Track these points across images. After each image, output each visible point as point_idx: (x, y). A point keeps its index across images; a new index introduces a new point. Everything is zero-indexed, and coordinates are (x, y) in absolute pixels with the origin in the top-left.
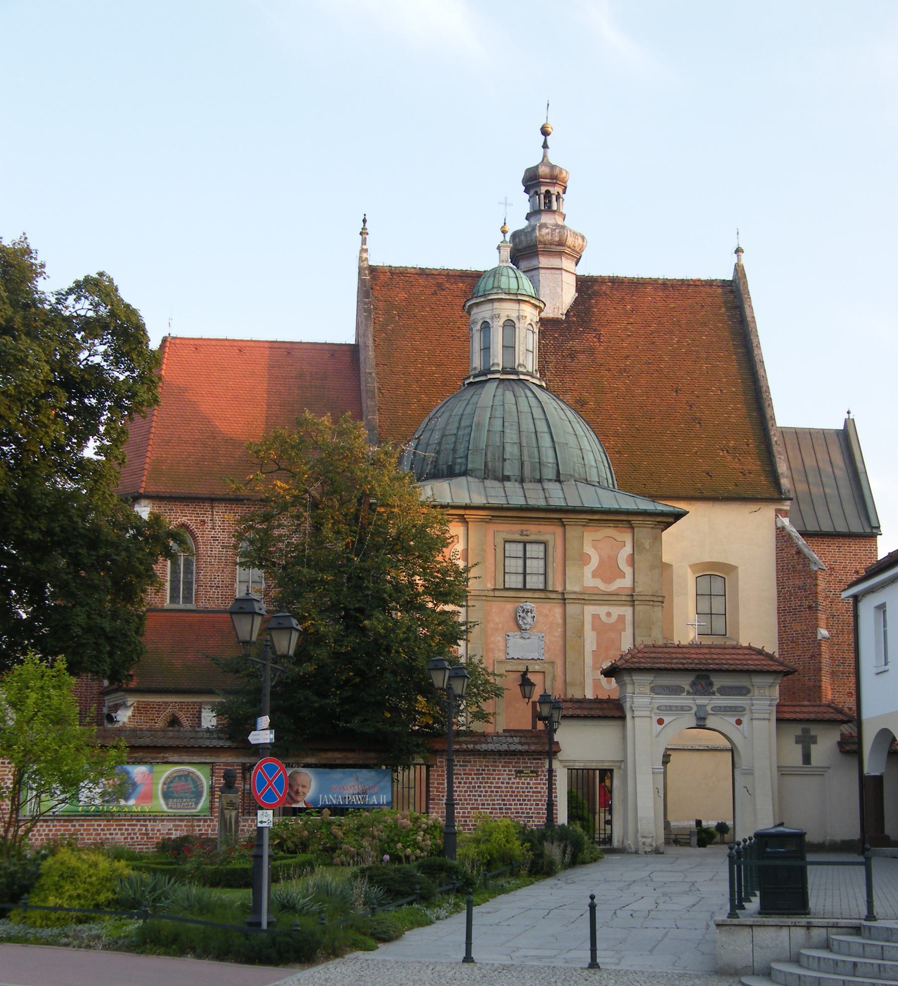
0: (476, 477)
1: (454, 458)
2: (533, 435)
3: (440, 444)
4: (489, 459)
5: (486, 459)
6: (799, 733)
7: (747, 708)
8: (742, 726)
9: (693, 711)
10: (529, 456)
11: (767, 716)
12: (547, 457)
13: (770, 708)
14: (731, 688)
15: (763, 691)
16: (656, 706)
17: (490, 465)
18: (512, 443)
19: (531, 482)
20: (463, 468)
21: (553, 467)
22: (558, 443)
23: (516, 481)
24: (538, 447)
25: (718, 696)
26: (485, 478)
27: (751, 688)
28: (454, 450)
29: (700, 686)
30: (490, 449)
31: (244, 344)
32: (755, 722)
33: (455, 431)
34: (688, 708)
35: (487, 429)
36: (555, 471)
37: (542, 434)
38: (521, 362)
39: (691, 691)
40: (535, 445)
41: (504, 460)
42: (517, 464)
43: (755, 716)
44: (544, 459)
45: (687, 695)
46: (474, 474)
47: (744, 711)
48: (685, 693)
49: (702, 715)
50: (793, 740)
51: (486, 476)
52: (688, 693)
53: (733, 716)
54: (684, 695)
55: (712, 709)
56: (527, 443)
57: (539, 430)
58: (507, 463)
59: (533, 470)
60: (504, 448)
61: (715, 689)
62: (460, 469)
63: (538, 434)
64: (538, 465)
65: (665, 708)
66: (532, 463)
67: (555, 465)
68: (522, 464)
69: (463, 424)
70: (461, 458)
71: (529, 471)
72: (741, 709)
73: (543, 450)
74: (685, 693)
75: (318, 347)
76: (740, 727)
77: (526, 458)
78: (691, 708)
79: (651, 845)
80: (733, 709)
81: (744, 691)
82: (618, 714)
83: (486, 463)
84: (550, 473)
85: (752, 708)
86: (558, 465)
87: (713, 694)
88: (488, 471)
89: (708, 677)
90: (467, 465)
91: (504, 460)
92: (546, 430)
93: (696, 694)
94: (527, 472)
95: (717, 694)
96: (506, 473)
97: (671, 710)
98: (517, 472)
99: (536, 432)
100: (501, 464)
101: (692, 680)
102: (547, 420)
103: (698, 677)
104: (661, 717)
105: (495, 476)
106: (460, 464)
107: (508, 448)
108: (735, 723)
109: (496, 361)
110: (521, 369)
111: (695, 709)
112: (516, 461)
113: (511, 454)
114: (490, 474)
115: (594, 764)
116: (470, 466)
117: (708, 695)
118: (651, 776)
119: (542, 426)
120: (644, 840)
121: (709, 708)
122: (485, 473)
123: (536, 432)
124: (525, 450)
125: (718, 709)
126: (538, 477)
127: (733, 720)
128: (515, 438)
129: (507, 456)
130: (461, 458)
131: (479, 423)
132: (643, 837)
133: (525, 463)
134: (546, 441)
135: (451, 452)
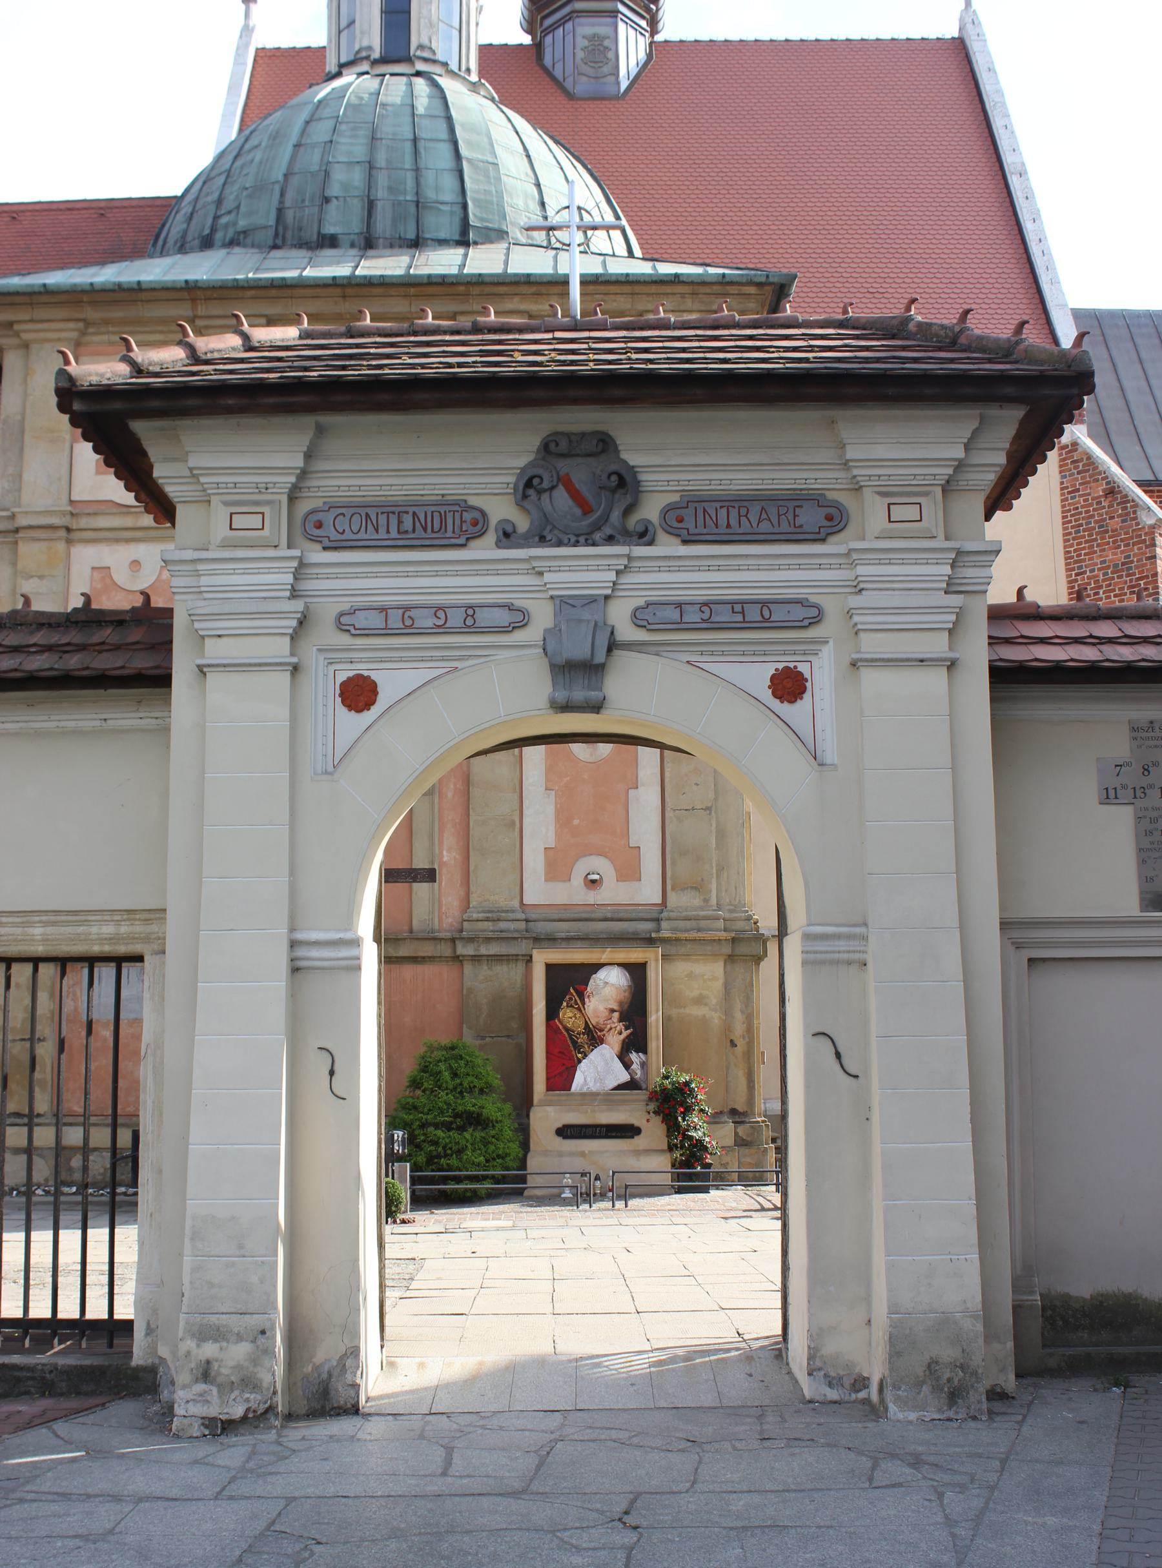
0: (253, 246)
1: (216, 218)
2: (408, 146)
3: (197, 199)
4: (288, 203)
5: (281, 202)
6: (1120, 747)
7: (831, 606)
8: (803, 705)
9: (533, 634)
10: (391, 189)
11: (938, 645)
12: (437, 189)
13: (956, 600)
14: (739, 502)
15: (912, 512)
16: (328, 610)
17: (289, 215)
18: (349, 164)
19: (391, 246)
20: (230, 234)
21: (452, 213)
22: (469, 161)
23: (352, 245)
24: (417, 170)
25: (667, 547)
26: (275, 247)
27: (844, 499)
28: (219, 202)
29: (561, 494)
30: (295, 181)
31: (22, 208)
32: (870, 678)
33: (227, 167)
34: (503, 617)
35: (294, 139)
36: (457, 221)
37: (431, 145)
38: (425, 42)
39: (523, 524)
40: (408, 163)
41: (327, 200)
42: (357, 208)
43: (872, 645)
44: (430, 194)
45: (499, 545)
46: (249, 241)
47: (817, 619)
48: (491, 537)
49: (578, 650)
50: (1092, 792)
51: (279, 242)
52: (507, 536)
53: (758, 654)
54: (484, 549)
55: (638, 618)
56: (388, 161)
57: (422, 134)
58: (332, 209)
59: (398, 219)
60: (327, 174)
61: (650, 510)
62: (225, 236)
63: (421, 145)
64: (413, 209)
65: (376, 621)
66: (396, 204)
67: (458, 209)
68: (371, 205)
69: (247, 147)
70: (229, 212)
71: (389, 222)
72: (798, 613)
73: (429, 177)
74: (491, 537)
75: (159, 203)
76: (795, 712)
77: (381, 193)
78: (520, 619)
79: (248, 1383)
80: (753, 614)
81: (810, 517)
82: (141, 662)
83: (280, 212)
84: (443, 224)
85: (855, 601)
86: (465, 206)
87: (644, 536)
88: (285, 228)
89: (605, 444)
90: (235, 224)
91: (327, 200)
92: (444, 134)
93: (542, 540)
94: (383, 224)
95: (662, 536)
96: (329, 229)
97: (410, 630)
98: (356, 225)
99: (415, 141)
100: (316, 209)
101: (522, 462)
102: (449, 119)
103: (548, 449)
104: (363, 669)
105: (300, 238)
106: (227, 226)
107: (339, 175)
108: (767, 695)
109: (365, 43)
110: (419, 53)
111: (543, 617)
112: (356, 201)
113: (346, 186)
114: (289, 234)
115: (38, 931)
116: (242, 223)
117: (610, 540)
118: (279, 983)
119: (434, 130)
120: (209, 1350)
121: (619, 615)
122: (276, 235)
123: (415, 141)
124: (382, 180)
125: (673, 614)
126: (411, 235)
127: (758, 676)
128: (360, 151)
129: (334, 190)
130: (229, 212)
131: (277, 133)
132: (205, 1334)
133: (379, 205)
134: (440, 157)
135: (213, 208)
